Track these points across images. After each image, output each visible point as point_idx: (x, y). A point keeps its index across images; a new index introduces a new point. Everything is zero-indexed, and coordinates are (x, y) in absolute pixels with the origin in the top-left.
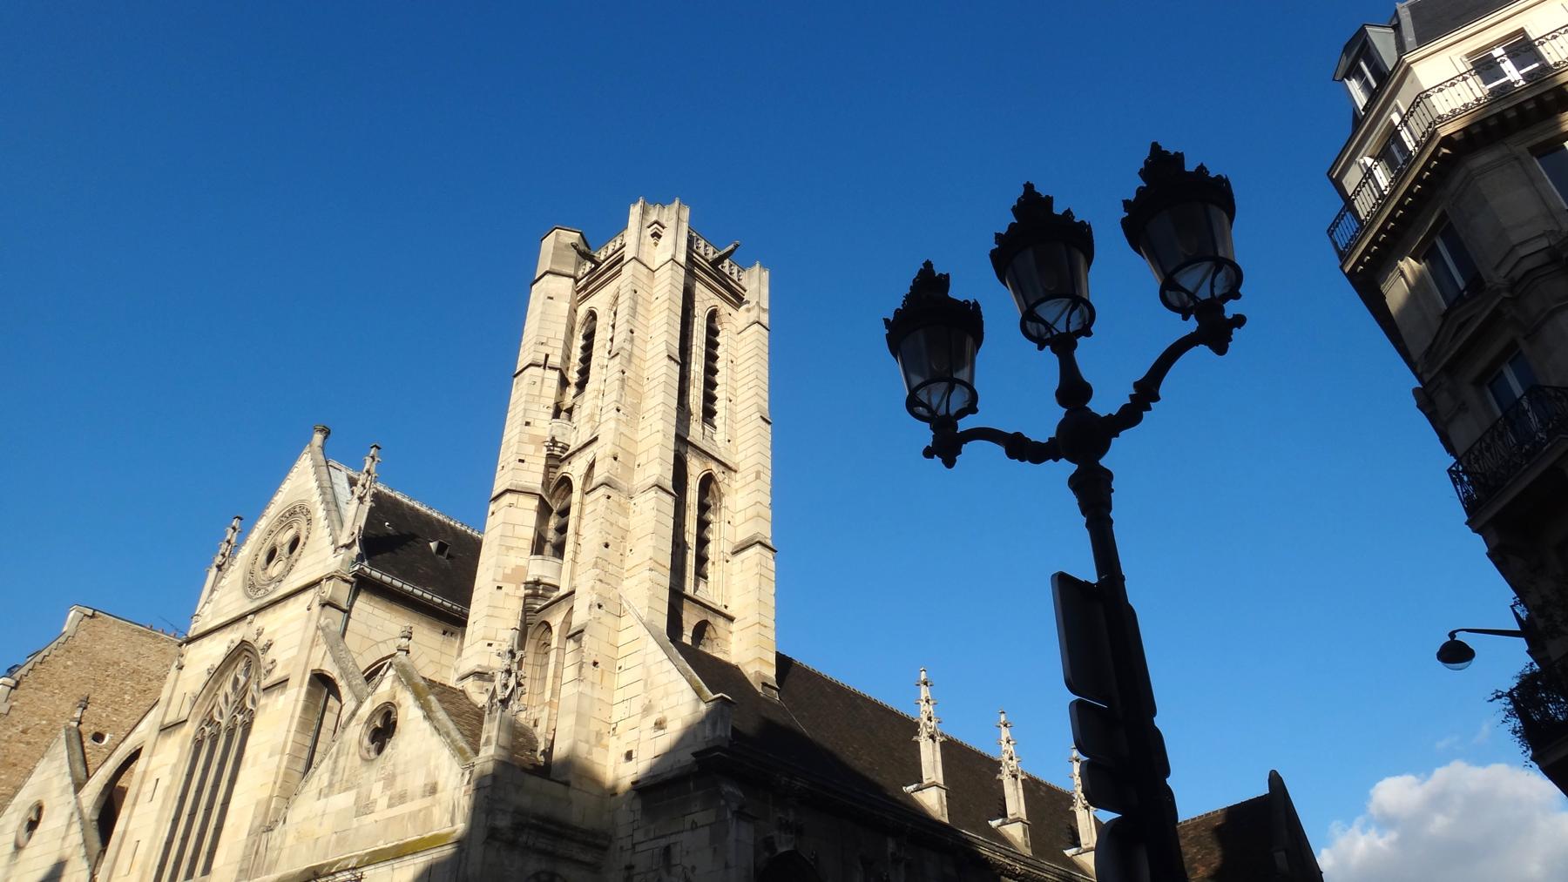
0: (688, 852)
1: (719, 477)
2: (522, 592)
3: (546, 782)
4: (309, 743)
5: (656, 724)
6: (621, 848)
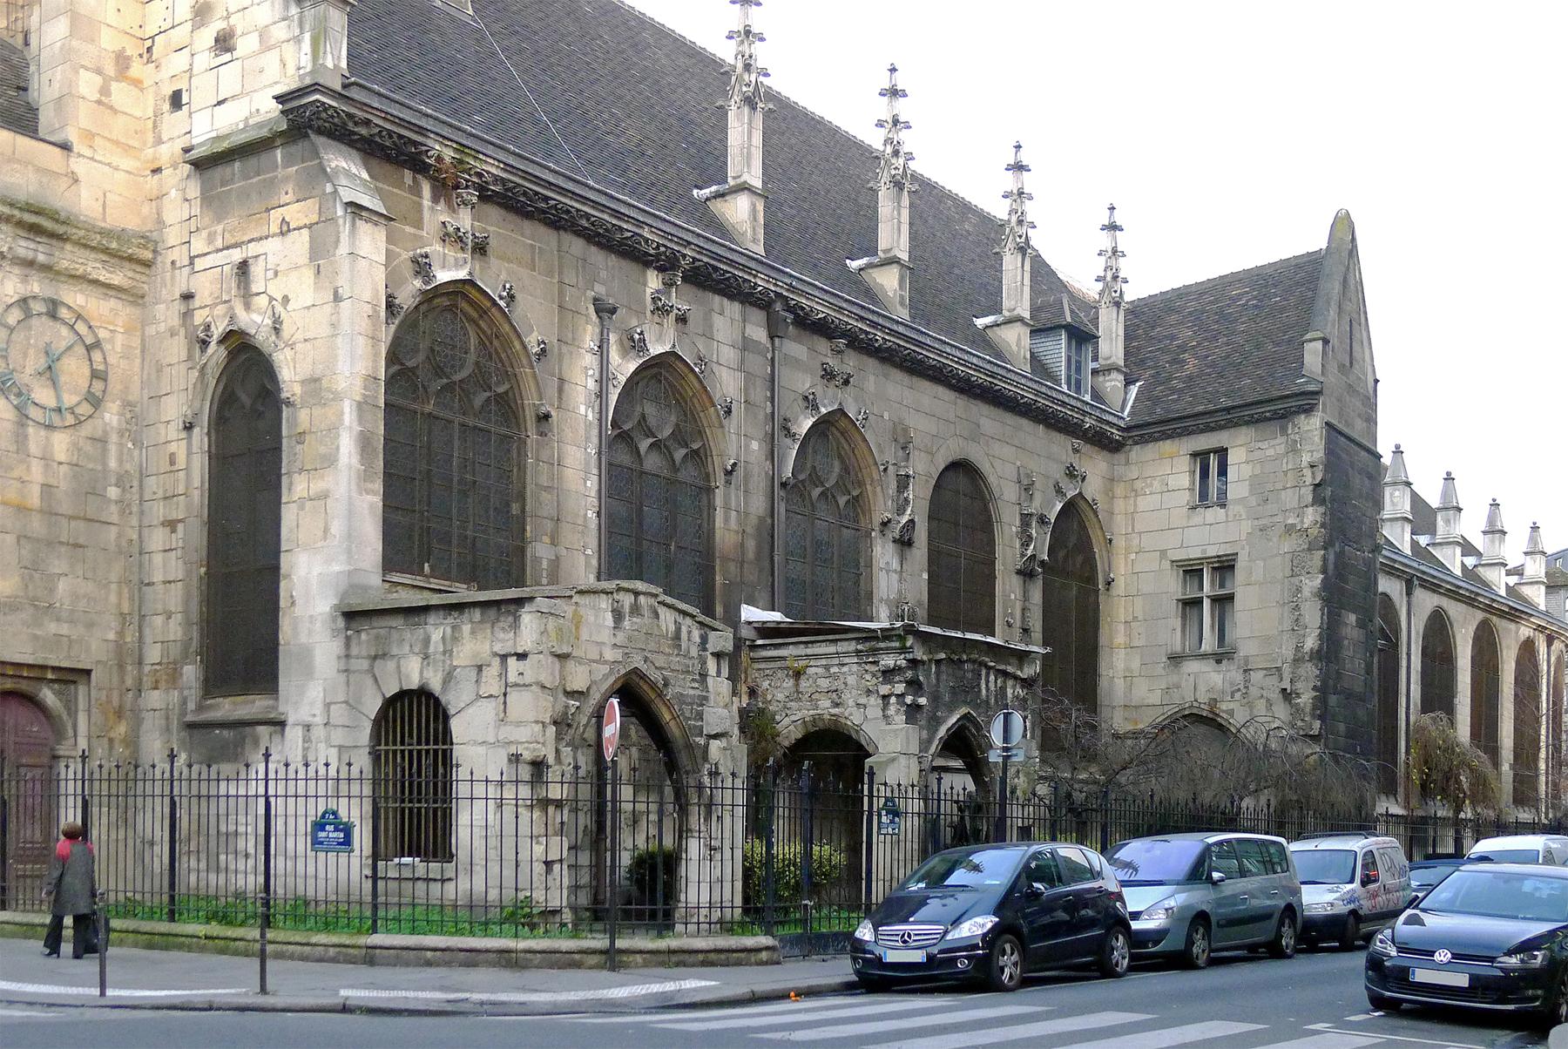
0: (276, 273)
3: (23, 142)
5: (217, 40)
6: (173, 263)
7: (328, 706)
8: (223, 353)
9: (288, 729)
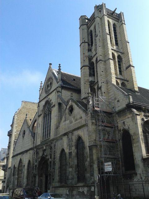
1: (121, 55)
2: (89, 83)
4: (60, 114)
7: (142, 171)
8: (122, 132)
9: (137, 175)
